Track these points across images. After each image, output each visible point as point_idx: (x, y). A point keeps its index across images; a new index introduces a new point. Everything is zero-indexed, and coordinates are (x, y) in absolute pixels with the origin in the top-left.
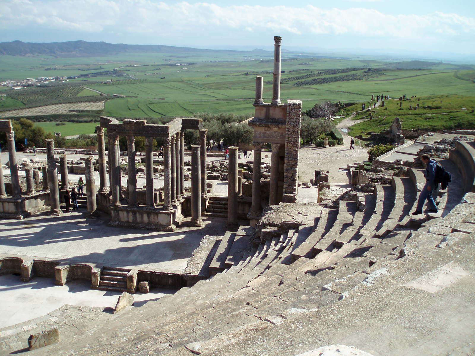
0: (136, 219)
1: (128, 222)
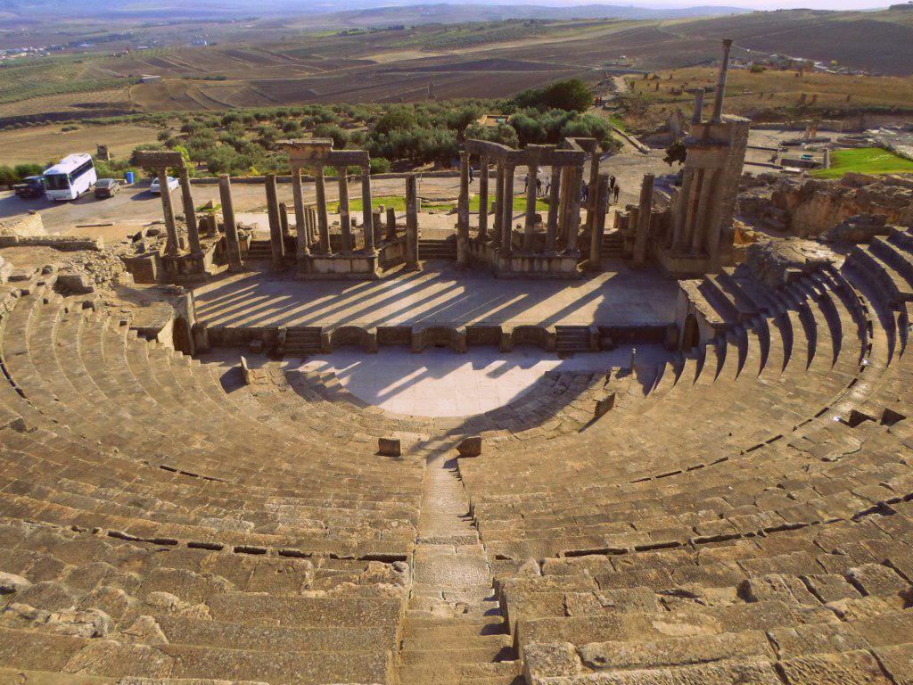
1: (522, 272)
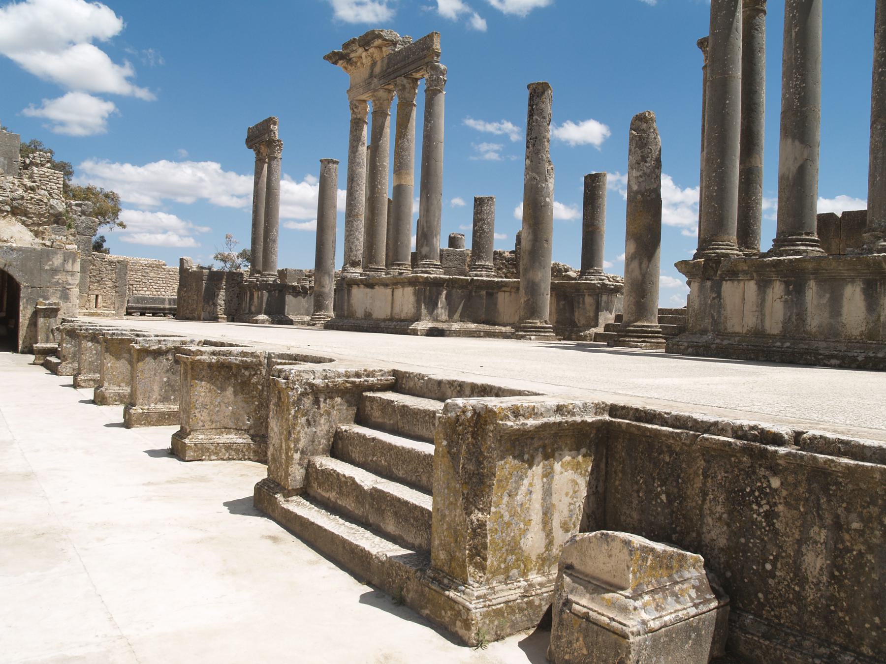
0: (801, 316)
1: (759, 333)
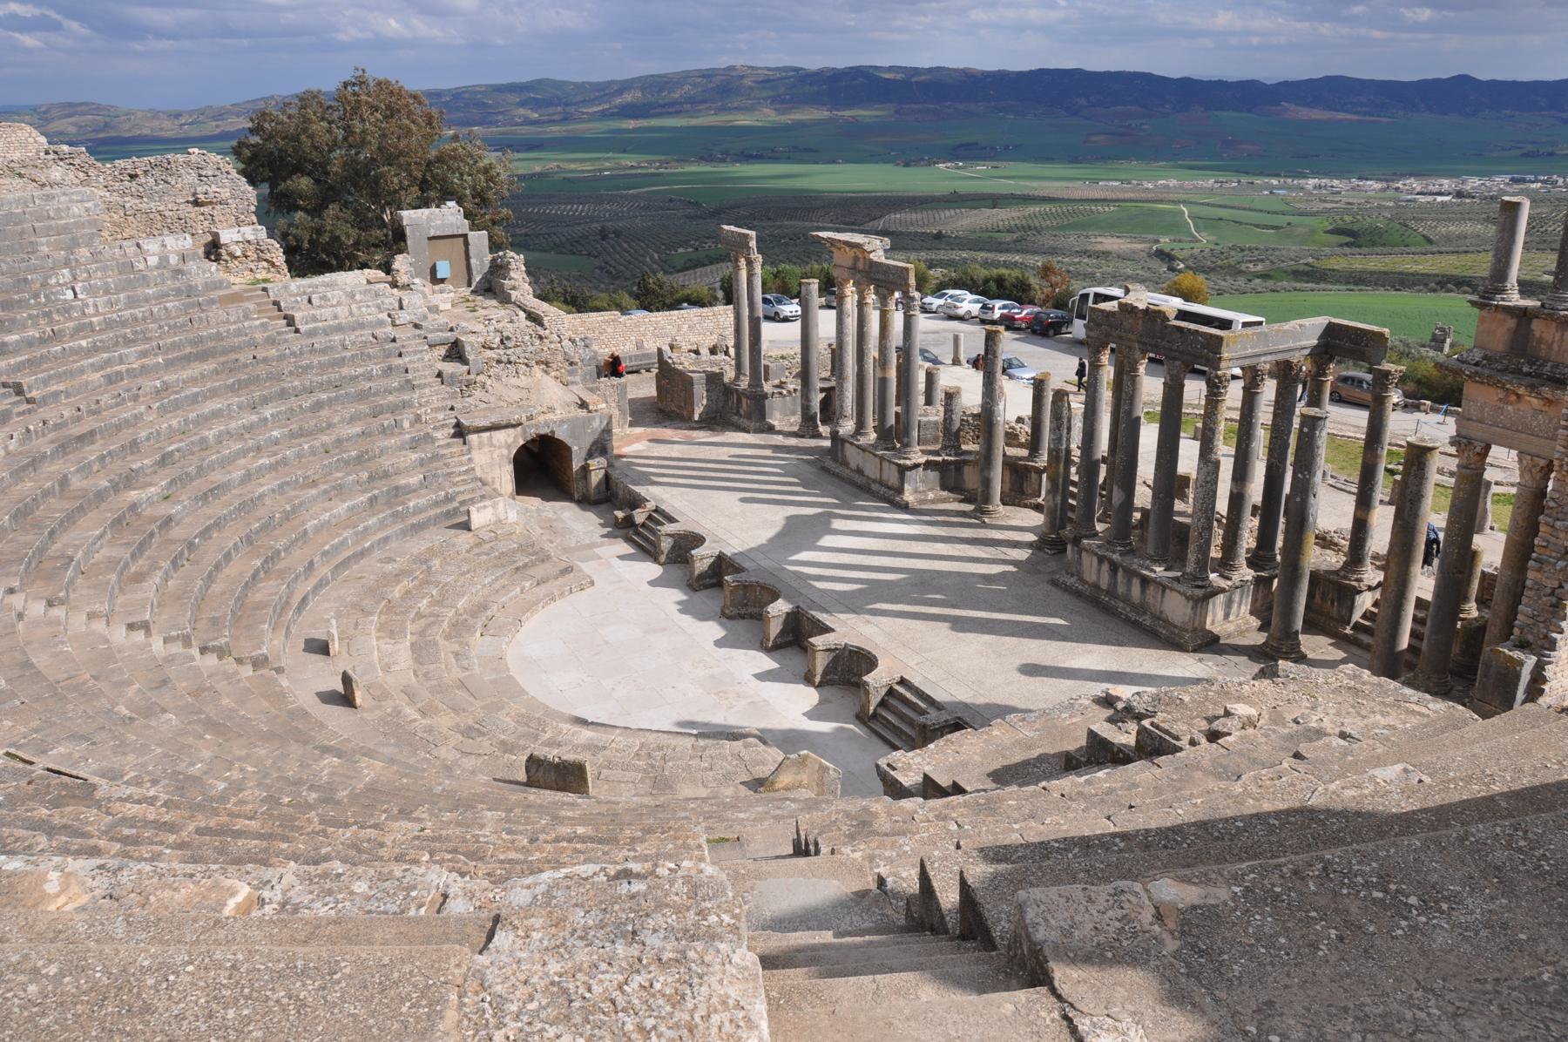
1: (1096, 586)
